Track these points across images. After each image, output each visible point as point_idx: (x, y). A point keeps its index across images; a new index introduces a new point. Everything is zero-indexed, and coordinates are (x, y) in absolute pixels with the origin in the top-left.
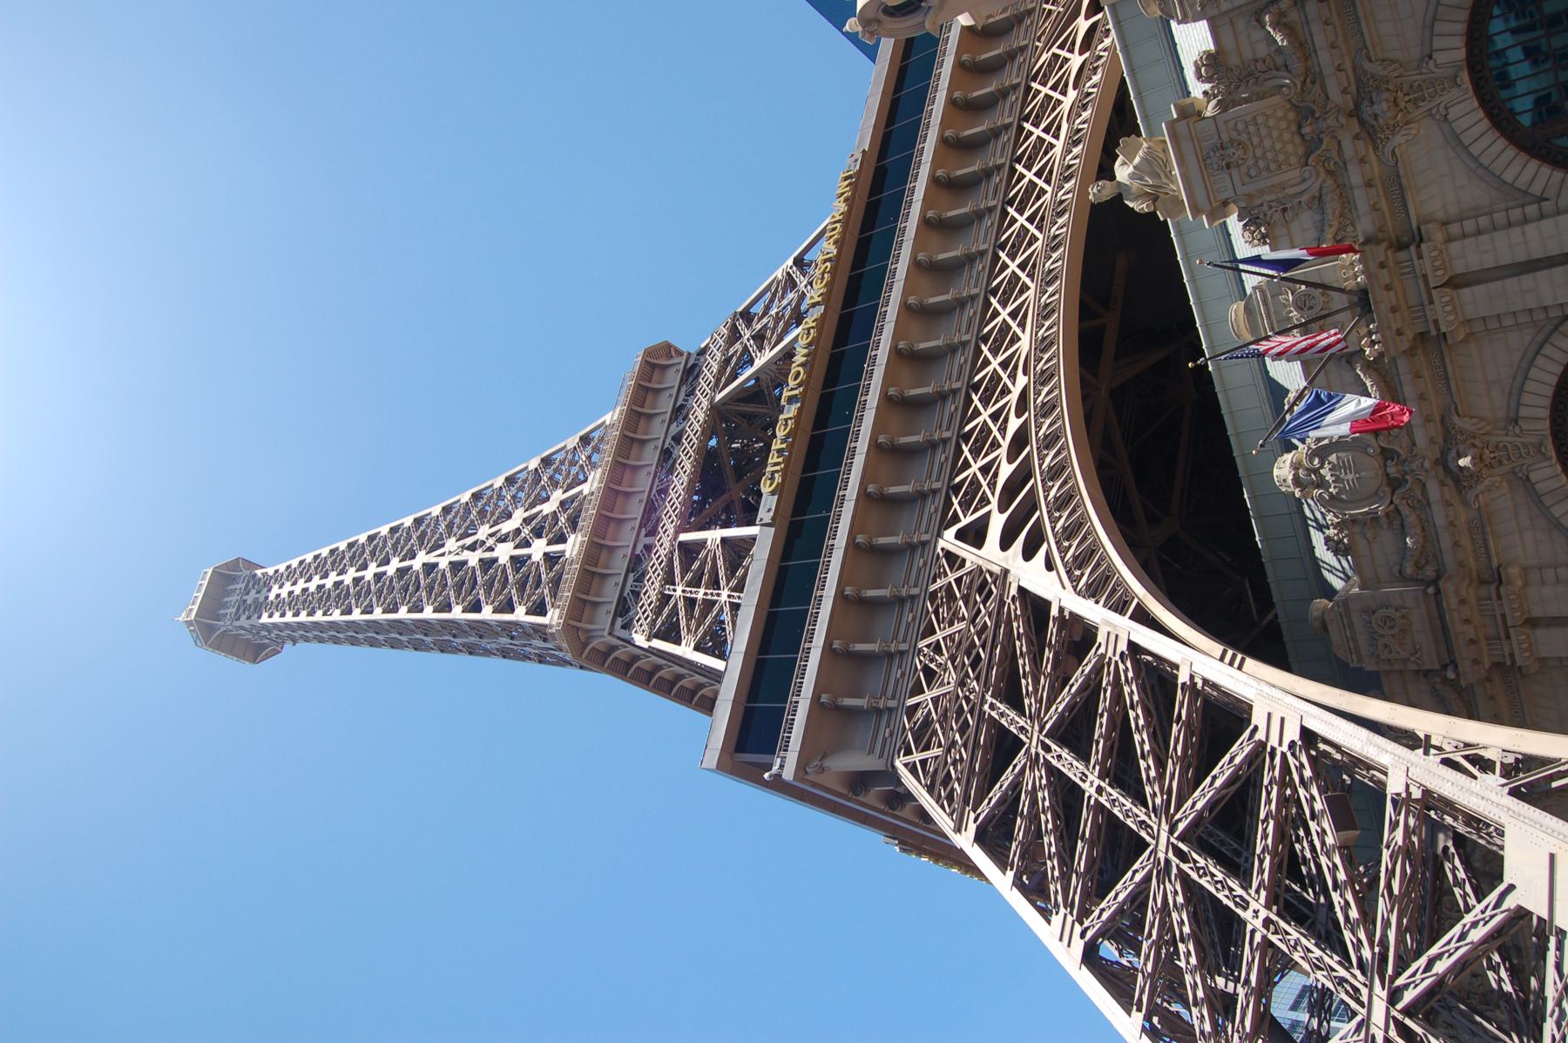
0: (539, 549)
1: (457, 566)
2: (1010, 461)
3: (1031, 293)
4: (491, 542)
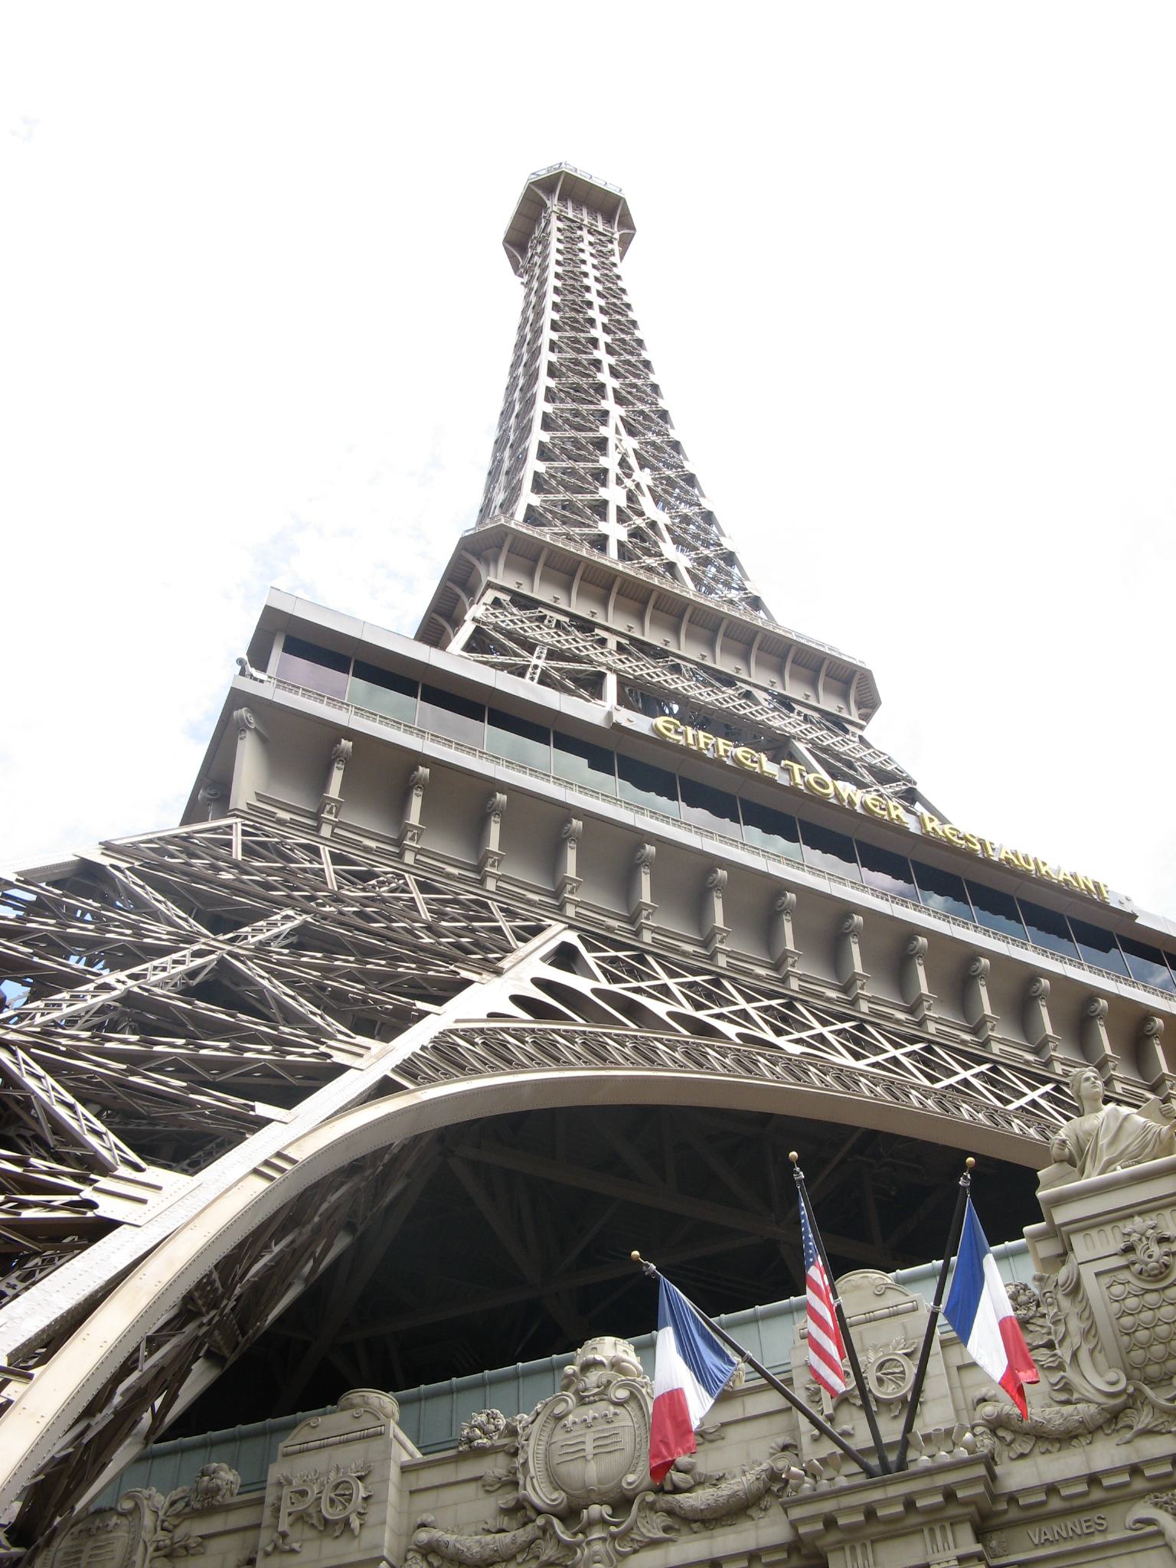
0: (615, 531)
1: (601, 444)
2: (670, 1014)
3: (927, 1083)
4: (628, 482)
